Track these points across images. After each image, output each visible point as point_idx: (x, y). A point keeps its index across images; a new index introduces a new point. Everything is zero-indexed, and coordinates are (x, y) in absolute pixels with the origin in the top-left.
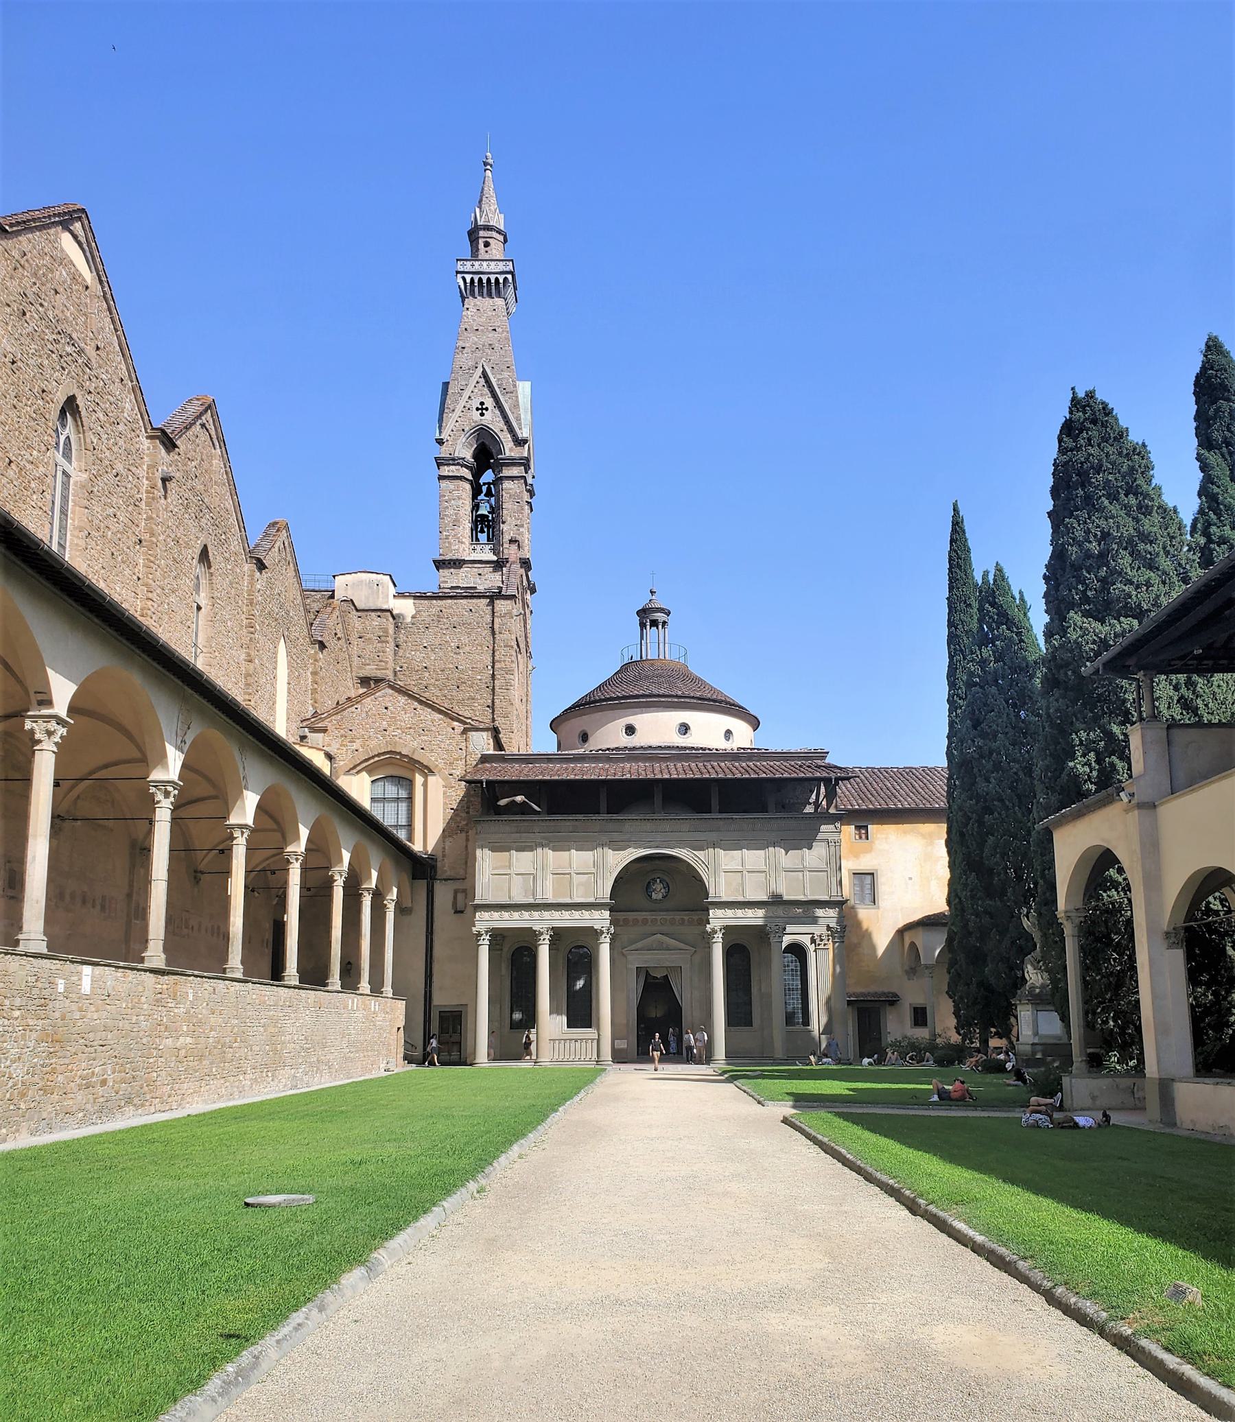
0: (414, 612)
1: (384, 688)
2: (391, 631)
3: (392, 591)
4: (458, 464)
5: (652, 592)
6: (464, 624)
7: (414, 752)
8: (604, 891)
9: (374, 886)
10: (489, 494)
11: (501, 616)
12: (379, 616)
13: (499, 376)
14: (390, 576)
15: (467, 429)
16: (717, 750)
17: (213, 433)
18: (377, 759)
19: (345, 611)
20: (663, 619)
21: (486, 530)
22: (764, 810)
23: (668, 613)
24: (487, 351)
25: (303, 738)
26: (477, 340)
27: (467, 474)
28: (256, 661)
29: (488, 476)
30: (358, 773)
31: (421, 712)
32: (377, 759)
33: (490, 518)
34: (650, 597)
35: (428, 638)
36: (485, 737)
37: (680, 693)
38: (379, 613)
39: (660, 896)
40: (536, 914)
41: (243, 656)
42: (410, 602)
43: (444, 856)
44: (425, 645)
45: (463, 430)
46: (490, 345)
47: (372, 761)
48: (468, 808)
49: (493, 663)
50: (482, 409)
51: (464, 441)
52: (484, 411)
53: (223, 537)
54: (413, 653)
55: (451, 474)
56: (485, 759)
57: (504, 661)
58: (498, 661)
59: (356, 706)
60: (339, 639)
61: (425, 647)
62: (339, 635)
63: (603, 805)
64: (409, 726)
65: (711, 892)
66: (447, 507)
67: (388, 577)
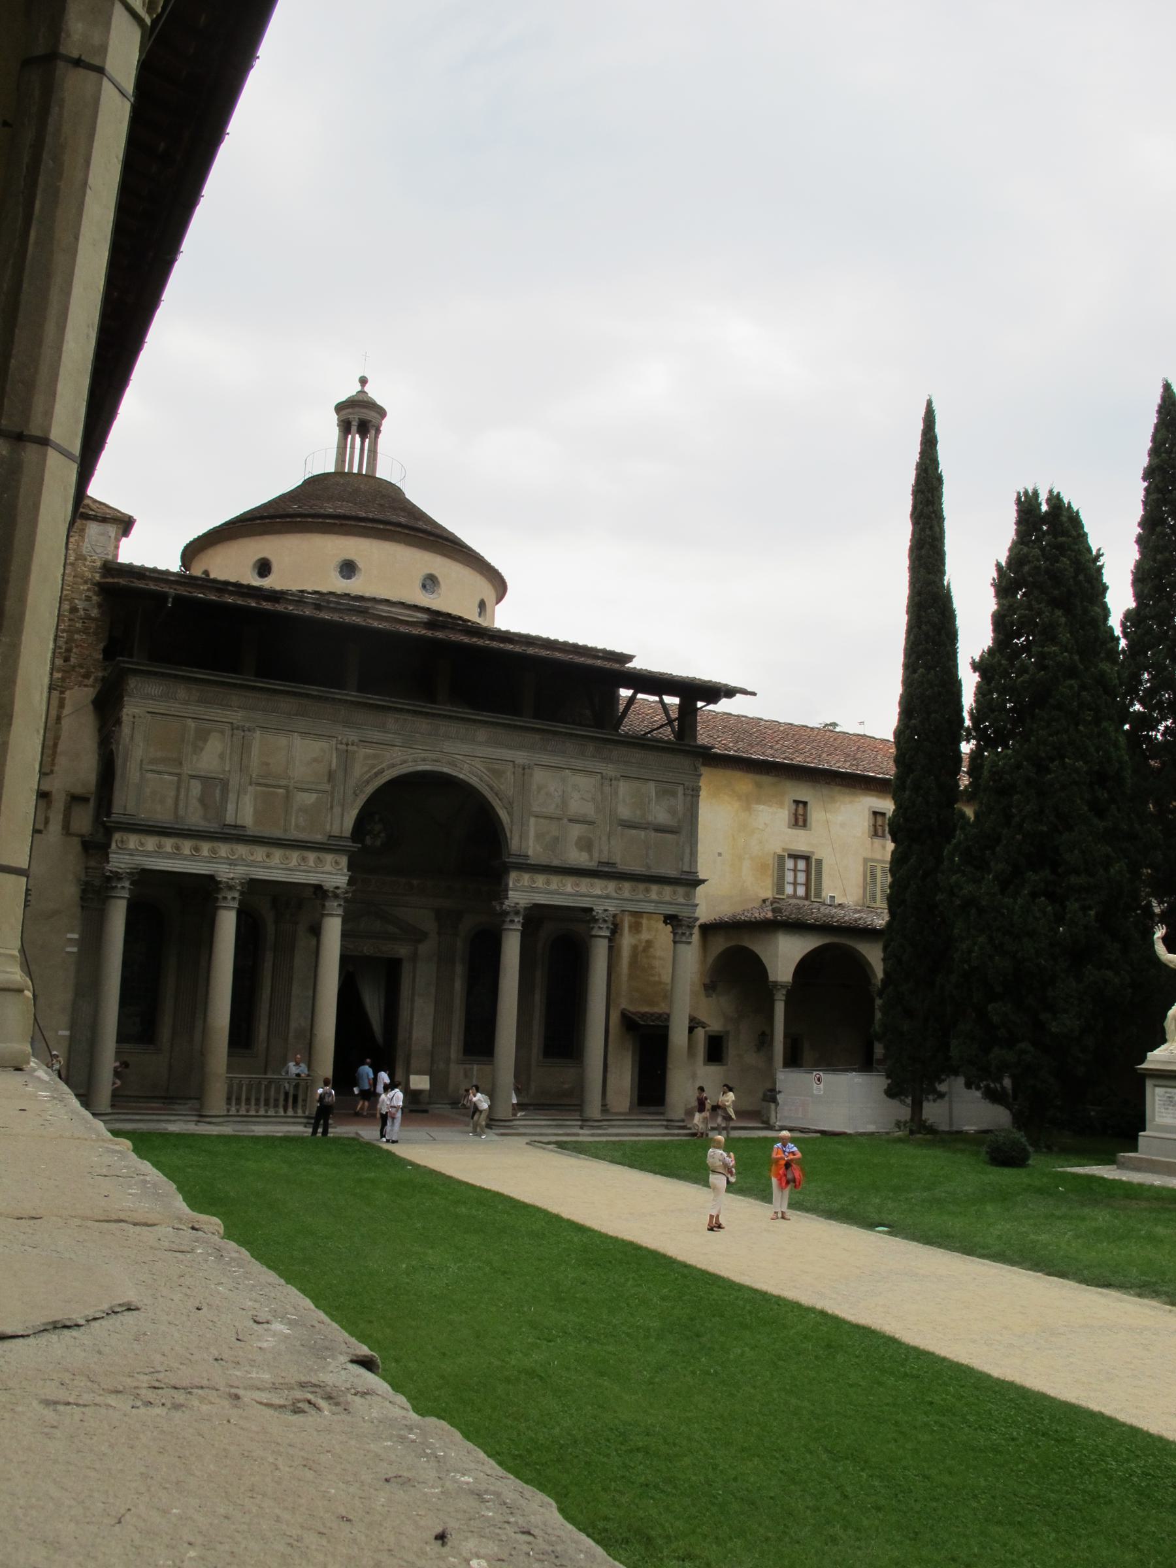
5: (363, 381)
39: (378, 843)
40: (224, 850)
48: (69, 650)
65: (514, 844)
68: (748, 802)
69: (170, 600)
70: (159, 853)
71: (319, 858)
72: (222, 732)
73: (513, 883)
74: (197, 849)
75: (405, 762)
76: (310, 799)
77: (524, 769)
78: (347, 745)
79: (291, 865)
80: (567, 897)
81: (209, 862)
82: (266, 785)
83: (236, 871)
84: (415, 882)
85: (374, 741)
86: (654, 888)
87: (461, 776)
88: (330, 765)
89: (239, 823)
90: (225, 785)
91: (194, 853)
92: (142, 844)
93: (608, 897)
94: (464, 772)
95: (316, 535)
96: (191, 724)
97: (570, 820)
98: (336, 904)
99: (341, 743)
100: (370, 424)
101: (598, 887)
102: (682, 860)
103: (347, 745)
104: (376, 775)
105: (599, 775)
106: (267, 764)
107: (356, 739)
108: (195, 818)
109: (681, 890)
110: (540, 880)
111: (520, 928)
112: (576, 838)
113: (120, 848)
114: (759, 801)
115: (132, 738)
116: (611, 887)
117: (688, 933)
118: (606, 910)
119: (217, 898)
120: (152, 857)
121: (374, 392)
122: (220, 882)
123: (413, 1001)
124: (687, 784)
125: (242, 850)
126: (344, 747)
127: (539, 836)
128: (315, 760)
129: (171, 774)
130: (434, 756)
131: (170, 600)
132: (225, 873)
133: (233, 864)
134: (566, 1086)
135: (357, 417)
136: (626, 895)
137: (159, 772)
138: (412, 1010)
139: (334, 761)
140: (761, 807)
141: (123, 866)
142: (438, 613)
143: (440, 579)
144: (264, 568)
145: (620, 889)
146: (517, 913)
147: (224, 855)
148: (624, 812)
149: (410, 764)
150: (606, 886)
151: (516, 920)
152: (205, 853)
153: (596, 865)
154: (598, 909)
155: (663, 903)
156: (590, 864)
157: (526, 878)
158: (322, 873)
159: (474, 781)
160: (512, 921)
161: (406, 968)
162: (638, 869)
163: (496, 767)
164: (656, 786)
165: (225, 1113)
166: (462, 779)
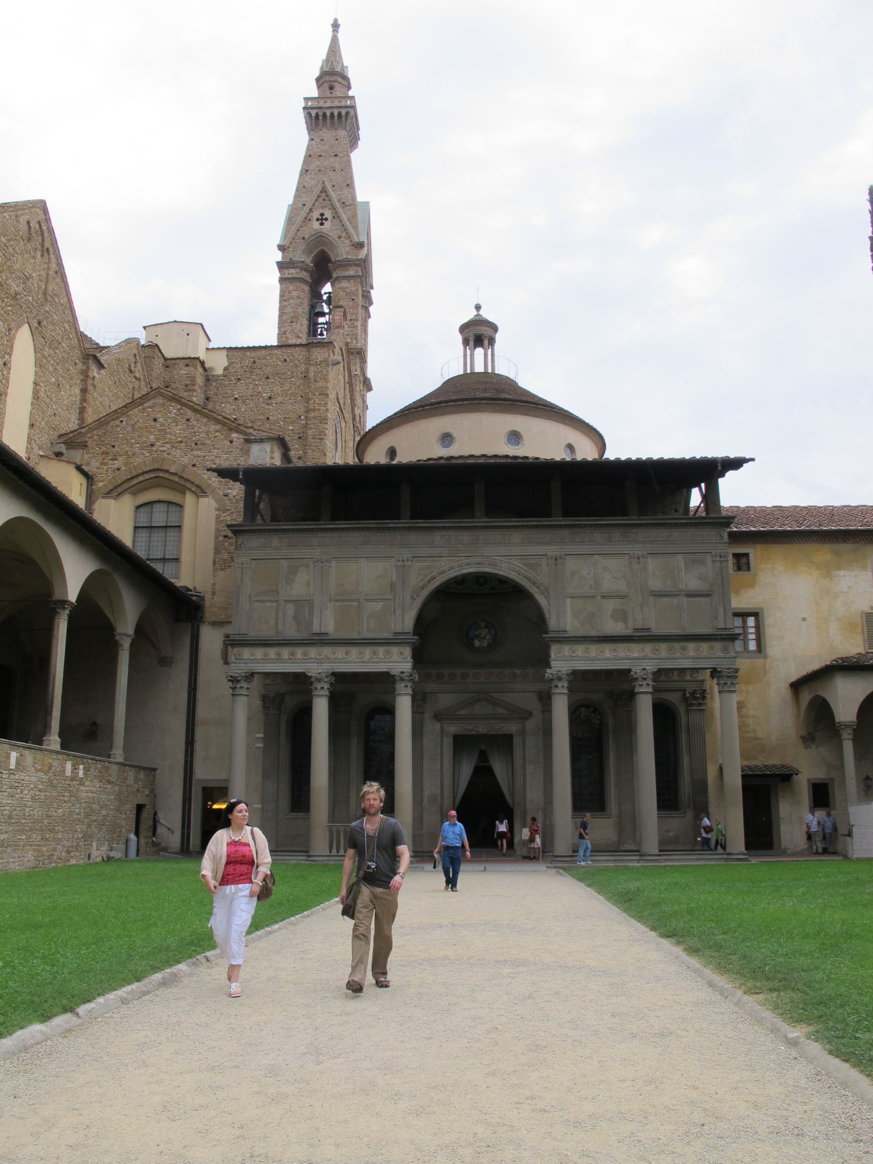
0: (226, 364)
1: (155, 397)
2: (200, 380)
4: (297, 267)
5: (478, 307)
6: (278, 374)
7: (183, 470)
8: (407, 621)
11: (316, 364)
12: (187, 365)
13: (338, 193)
15: (306, 237)
18: (141, 478)
19: (149, 357)
24: (328, 172)
26: (320, 164)
30: (119, 495)
31: (195, 423)
32: (141, 478)
34: (476, 313)
36: (268, 450)
38: (187, 361)
39: (485, 644)
40: (313, 652)
43: (214, 593)
44: (236, 396)
45: (304, 238)
46: (332, 167)
47: (135, 481)
49: (308, 411)
50: (322, 220)
51: (304, 247)
52: (324, 221)
54: (223, 405)
55: (289, 276)
57: (319, 410)
58: (314, 410)
59: (121, 419)
60: (135, 378)
61: (236, 399)
62: (137, 375)
64: (179, 439)
65: (553, 623)
66: (286, 306)
67: (200, 326)
68: (827, 571)
69: (241, 473)
70: (266, 660)
71: (386, 651)
72: (307, 566)
73: (555, 655)
74: (293, 654)
75: (452, 568)
76: (377, 606)
77: (556, 560)
78: (403, 561)
79: (365, 659)
80: (605, 662)
81: (304, 663)
82: (343, 601)
83: (323, 667)
84: (518, 672)
85: (425, 555)
86: (691, 646)
87: (501, 573)
88: (392, 580)
89: (323, 631)
90: (310, 603)
91: (291, 657)
93: (644, 658)
94: (503, 569)
95: (422, 420)
96: (284, 563)
97: (604, 597)
98: (403, 685)
99: (399, 561)
100: (483, 337)
101: (636, 650)
102: (716, 619)
103: (403, 561)
104: (429, 581)
105: (627, 557)
106: (343, 585)
107: (410, 556)
108: (291, 631)
109: (718, 645)
110: (580, 650)
111: (566, 692)
112: (611, 611)
113: (238, 659)
114: (839, 568)
115: (242, 579)
116: (648, 648)
117: (729, 683)
118: (644, 669)
119: (311, 689)
120: (260, 663)
121: (486, 314)
122: (310, 677)
123: (524, 768)
124: (713, 552)
125: (327, 651)
126: (401, 563)
129: (271, 601)
130: (477, 560)
131: (241, 473)
132: (313, 669)
133: (320, 662)
134: (671, 834)
135: (472, 334)
136: (664, 654)
137: (262, 601)
138: (524, 776)
139: (394, 575)
140: (842, 573)
141: (239, 672)
143: (522, 433)
144: (392, 452)
145: (657, 650)
147: (313, 656)
148: (655, 584)
149: (457, 569)
150: (643, 649)
151: (560, 685)
152: (299, 656)
153: (631, 631)
154: (637, 670)
155: (701, 658)
156: (626, 632)
157: (566, 649)
158: (390, 662)
159: (513, 576)
160: (556, 686)
161: (517, 741)
163: (532, 561)
164: (684, 559)
165: (328, 853)
166: (502, 576)
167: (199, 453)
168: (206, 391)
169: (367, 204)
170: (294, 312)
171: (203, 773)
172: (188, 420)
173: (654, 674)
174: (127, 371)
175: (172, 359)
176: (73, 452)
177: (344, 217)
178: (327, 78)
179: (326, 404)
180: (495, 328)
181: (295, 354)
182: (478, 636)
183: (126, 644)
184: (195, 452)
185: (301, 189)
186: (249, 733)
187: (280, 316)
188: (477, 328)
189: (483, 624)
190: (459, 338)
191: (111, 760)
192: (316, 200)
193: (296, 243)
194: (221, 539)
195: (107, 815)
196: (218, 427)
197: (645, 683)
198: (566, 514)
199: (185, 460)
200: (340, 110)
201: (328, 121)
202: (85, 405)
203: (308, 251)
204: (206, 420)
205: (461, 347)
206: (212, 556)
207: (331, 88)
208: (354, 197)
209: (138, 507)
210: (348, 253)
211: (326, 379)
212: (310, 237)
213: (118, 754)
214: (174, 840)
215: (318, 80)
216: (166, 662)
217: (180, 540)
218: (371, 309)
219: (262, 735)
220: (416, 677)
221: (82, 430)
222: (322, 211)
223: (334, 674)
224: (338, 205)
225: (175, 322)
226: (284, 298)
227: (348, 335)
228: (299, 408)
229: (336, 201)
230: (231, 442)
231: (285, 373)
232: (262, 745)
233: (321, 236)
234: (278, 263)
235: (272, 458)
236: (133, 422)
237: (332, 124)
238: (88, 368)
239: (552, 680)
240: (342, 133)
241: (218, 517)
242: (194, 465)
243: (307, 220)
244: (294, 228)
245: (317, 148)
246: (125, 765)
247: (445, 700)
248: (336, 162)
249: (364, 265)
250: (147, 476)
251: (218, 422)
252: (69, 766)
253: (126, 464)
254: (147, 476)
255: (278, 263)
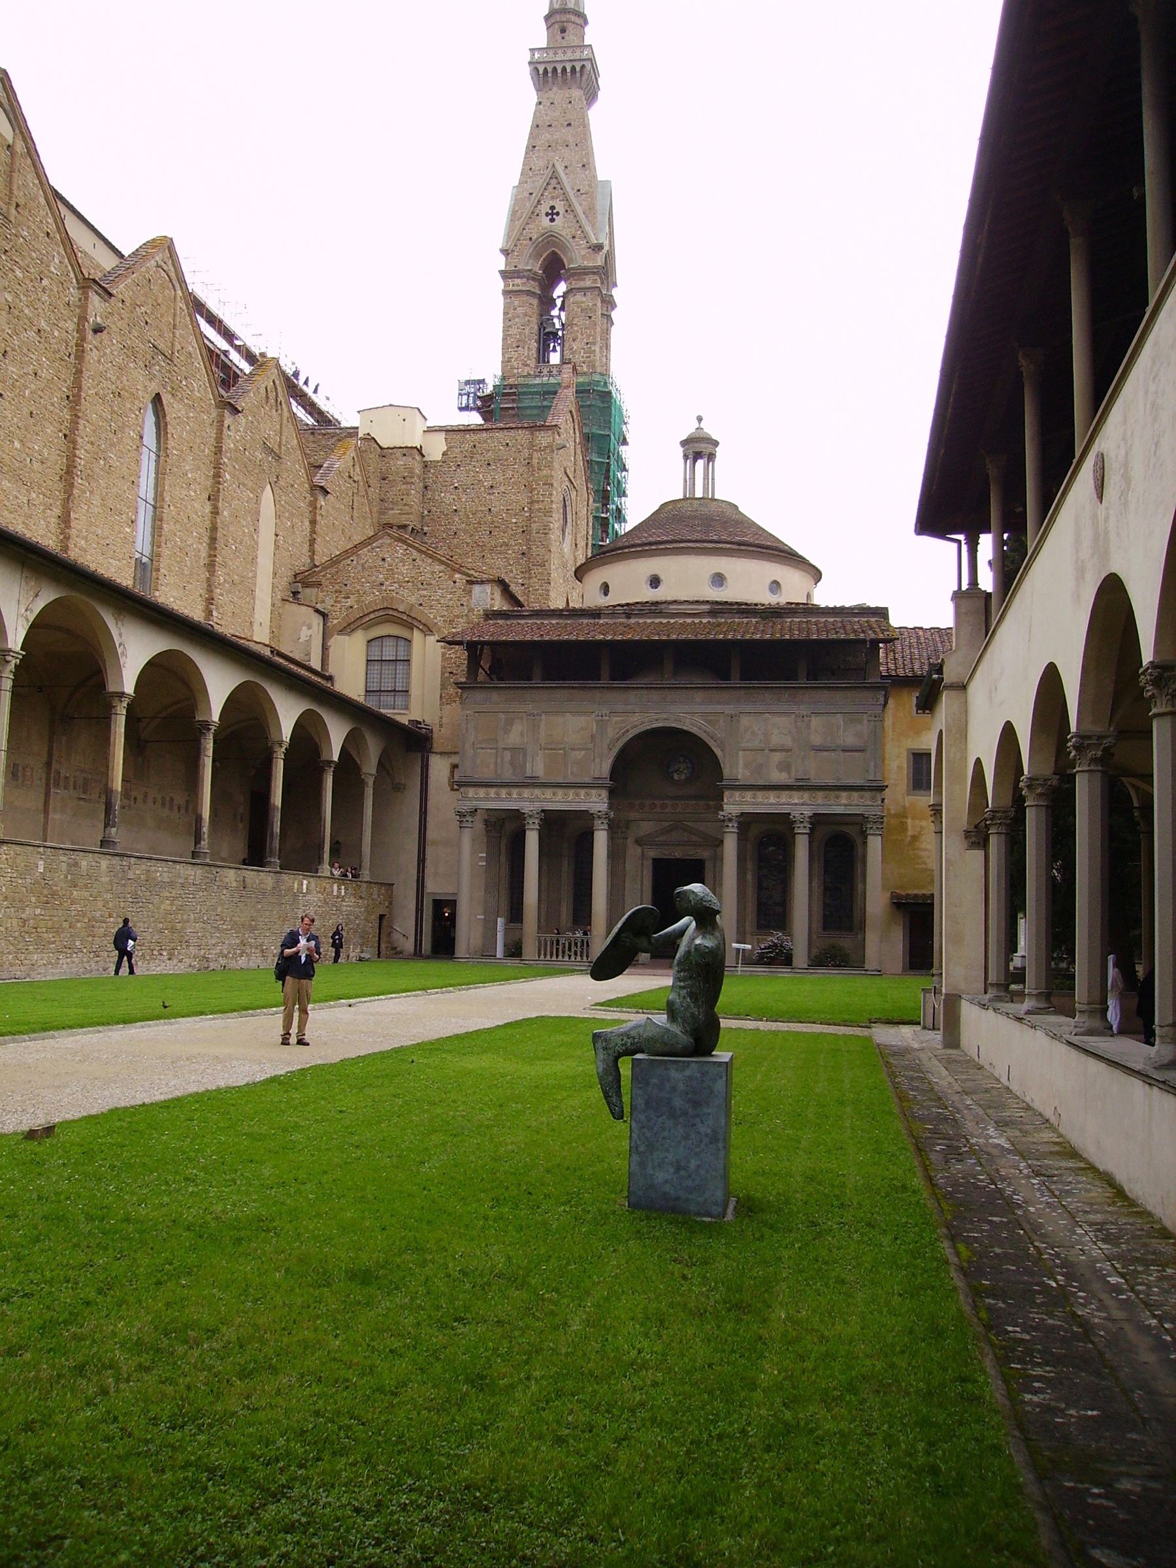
0: (445, 448)
3: (421, 426)
5: (700, 419)
7: (411, 609)
8: (604, 768)
9: (336, 758)
10: (562, 308)
12: (405, 455)
14: (419, 410)
16: (756, 605)
17: (173, 275)
18: (372, 616)
20: (708, 451)
21: (558, 348)
22: (791, 676)
23: (716, 444)
25: (295, 593)
27: (534, 287)
28: (225, 513)
29: (561, 289)
31: (420, 563)
32: (372, 616)
33: (560, 333)
35: (460, 478)
36: (489, 592)
37: (715, 538)
39: (683, 777)
40: (526, 793)
41: (208, 508)
42: (443, 435)
43: (441, 726)
44: (456, 485)
45: (531, 239)
49: (532, 503)
50: (552, 214)
53: (184, 383)
56: (490, 615)
57: (543, 501)
58: (538, 502)
60: (355, 481)
62: (356, 479)
63: (605, 670)
65: (726, 772)
70: (487, 799)
72: (522, 719)
76: (580, 755)
86: (844, 794)
87: (685, 728)
92: (476, 794)
96: (502, 716)
97: (771, 750)
101: (796, 797)
105: (793, 716)
108: (508, 775)
109: (867, 794)
110: (748, 796)
115: (467, 730)
122: (524, 814)
125: (537, 792)
127: (746, 766)
128: (582, 729)
130: (665, 716)
132: (526, 807)
135: (691, 451)
136: (820, 801)
142: (717, 603)
143: (726, 575)
144: (605, 589)
146: (730, 820)
148: (816, 740)
152: (515, 796)
154: (795, 813)
159: (694, 730)
161: (708, 866)
162: (831, 782)
167: (425, 592)
168: (424, 479)
169: (608, 182)
170: (520, 334)
171: (435, 887)
172: (414, 560)
173: (810, 817)
174: (347, 479)
175: (388, 448)
176: (308, 591)
177: (579, 210)
178: (558, 17)
179: (551, 495)
180: (716, 444)
181: (517, 437)
182: (677, 771)
183: (370, 782)
184: (421, 592)
185: (528, 170)
186: (473, 852)
187: (504, 339)
188: (696, 445)
189: (681, 759)
190: (680, 451)
191: (360, 879)
192: (545, 189)
193: (521, 244)
194: (447, 675)
195: (359, 924)
196: (442, 567)
197: (802, 825)
198: (745, 677)
199: (413, 600)
200: (574, 63)
201: (560, 79)
202: (315, 536)
203: (536, 255)
204: (431, 560)
205: (682, 461)
206: (439, 691)
207: (563, 31)
208: (595, 176)
209: (369, 642)
210: (584, 258)
211: (550, 466)
212: (537, 239)
213: (366, 875)
214: (409, 946)
215: (547, 18)
216: (399, 788)
217: (408, 674)
218: (614, 315)
219: (484, 855)
220: (612, 814)
221: (316, 569)
222: (552, 203)
223: (543, 811)
224: (571, 194)
225: (391, 405)
226: (508, 317)
227: (584, 363)
228: (523, 499)
229: (568, 189)
230: (455, 582)
231: (507, 460)
232: (484, 863)
233: (552, 236)
234: (501, 272)
235: (492, 599)
236: (363, 561)
237: (565, 81)
238: (316, 500)
239: (724, 821)
240: (576, 93)
241: (443, 655)
242: (421, 605)
243: (534, 215)
244: (518, 224)
245: (547, 115)
246: (371, 883)
247: (646, 828)
248: (568, 134)
249: (606, 273)
250: (377, 614)
251: (442, 563)
252: (335, 887)
253: (358, 602)
254: (377, 614)
255: (501, 272)
